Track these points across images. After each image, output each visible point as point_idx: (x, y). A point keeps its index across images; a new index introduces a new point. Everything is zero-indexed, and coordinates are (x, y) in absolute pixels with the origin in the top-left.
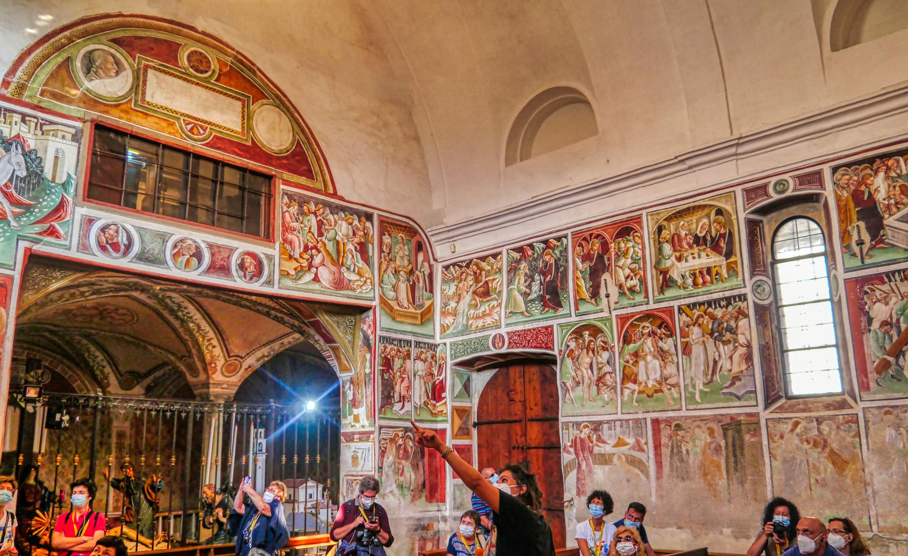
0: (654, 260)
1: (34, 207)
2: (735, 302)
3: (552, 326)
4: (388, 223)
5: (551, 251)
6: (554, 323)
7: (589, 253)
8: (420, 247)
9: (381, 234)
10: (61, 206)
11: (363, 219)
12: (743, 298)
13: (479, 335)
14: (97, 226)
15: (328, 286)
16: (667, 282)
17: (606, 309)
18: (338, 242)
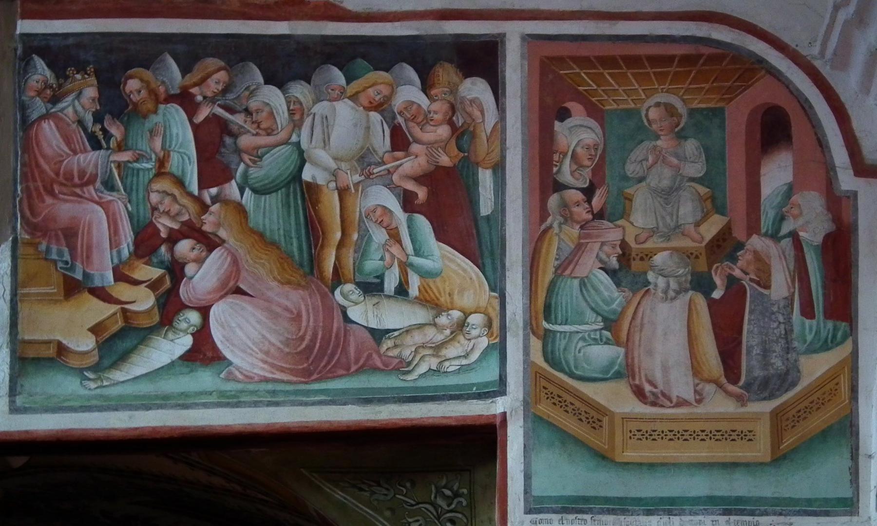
4: (584, 62)
8: (774, 129)
9: (548, 112)
11: (446, 73)
15: (260, 370)
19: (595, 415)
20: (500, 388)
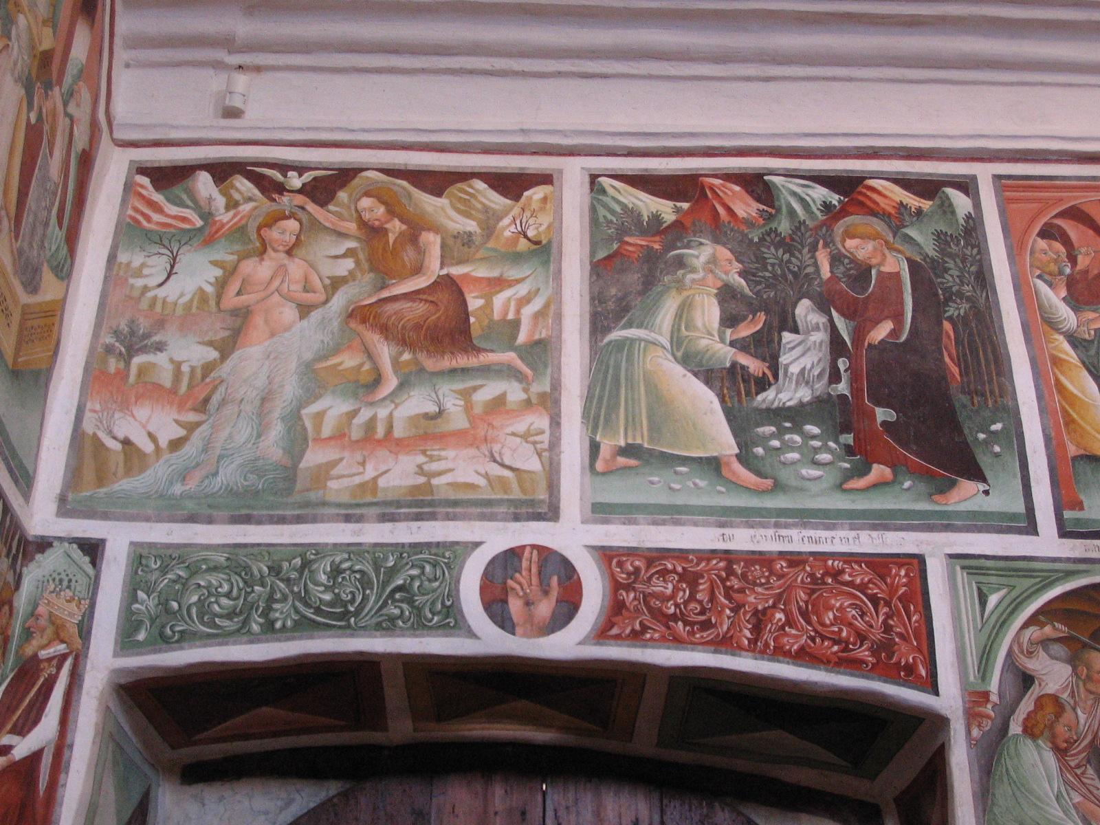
3: (917, 563)
5: (878, 225)
6: (935, 547)
13: (374, 533)
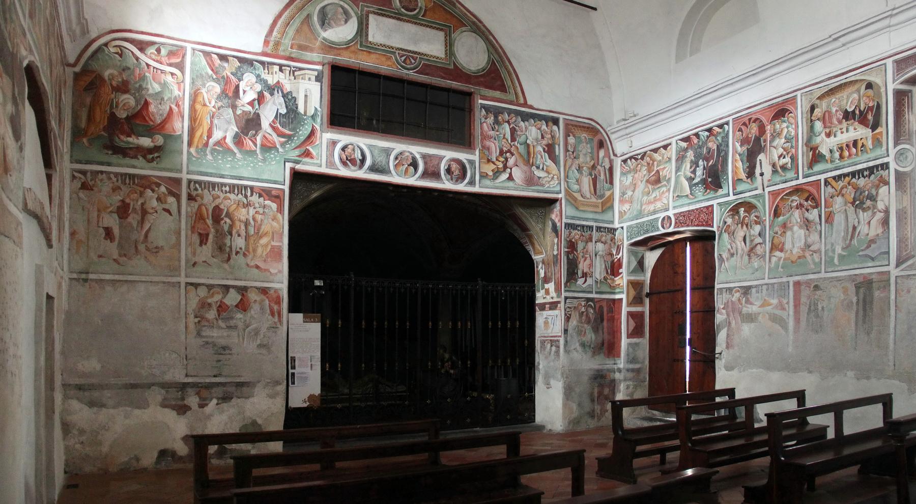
0: (805, 138)
1: (294, 136)
2: (878, 170)
7: (747, 137)
8: (601, 144)
10: (312, 133)
12: (885, 166)
14: (339, 146)
16: (816, 157)
17: (760, 187)
18: (528, 146)
19: (575, 199)
20: (560, 192)
